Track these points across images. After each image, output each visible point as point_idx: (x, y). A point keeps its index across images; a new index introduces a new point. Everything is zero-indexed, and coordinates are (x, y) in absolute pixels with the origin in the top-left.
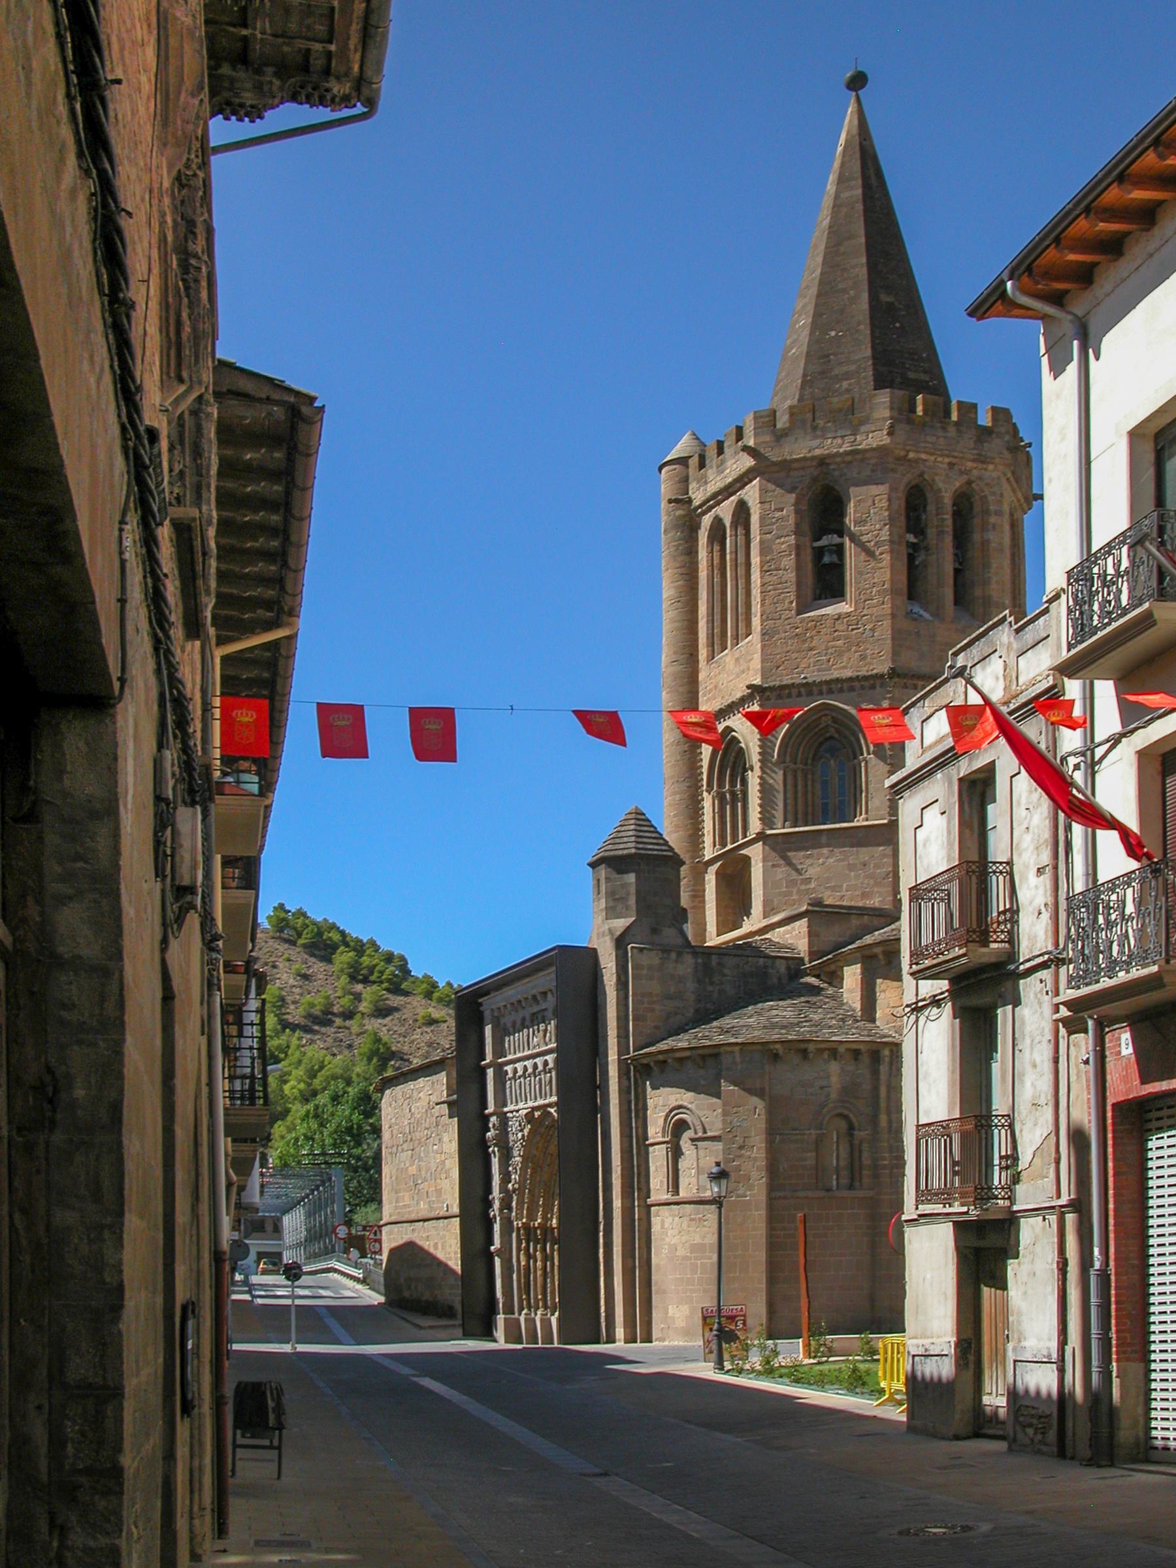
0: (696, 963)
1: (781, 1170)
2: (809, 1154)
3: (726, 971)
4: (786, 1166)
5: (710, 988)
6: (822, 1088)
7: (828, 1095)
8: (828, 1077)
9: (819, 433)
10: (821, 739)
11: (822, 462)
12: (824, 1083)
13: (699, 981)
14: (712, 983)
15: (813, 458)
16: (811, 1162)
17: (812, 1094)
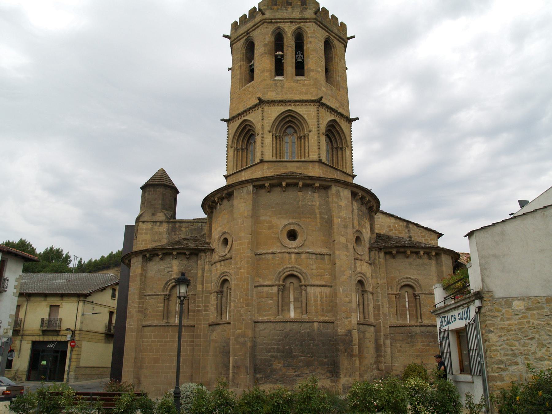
0: (168, 227)
1: (148, 312)
2: (161, 305)
3: (182, 229)
4: (150, 310)
5: (175, 237)
6: (168, 272)
7: (171, 276)
8: (172, 267)
9: (246, 23)
10: (249, 136)
11: (247, 33)
12: (170, 270)
13: (169, 234)
14: (175, 235)
15: (244, 33)
16: (161, 309)
17: (163, 276)
